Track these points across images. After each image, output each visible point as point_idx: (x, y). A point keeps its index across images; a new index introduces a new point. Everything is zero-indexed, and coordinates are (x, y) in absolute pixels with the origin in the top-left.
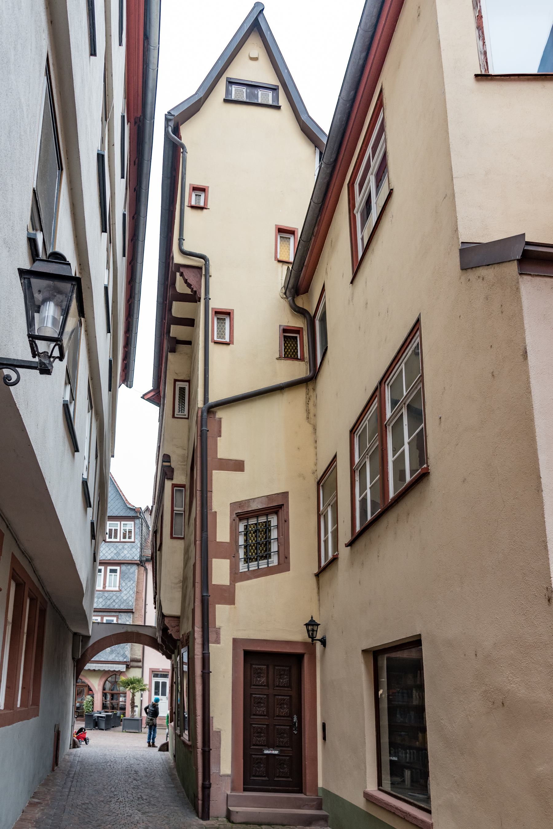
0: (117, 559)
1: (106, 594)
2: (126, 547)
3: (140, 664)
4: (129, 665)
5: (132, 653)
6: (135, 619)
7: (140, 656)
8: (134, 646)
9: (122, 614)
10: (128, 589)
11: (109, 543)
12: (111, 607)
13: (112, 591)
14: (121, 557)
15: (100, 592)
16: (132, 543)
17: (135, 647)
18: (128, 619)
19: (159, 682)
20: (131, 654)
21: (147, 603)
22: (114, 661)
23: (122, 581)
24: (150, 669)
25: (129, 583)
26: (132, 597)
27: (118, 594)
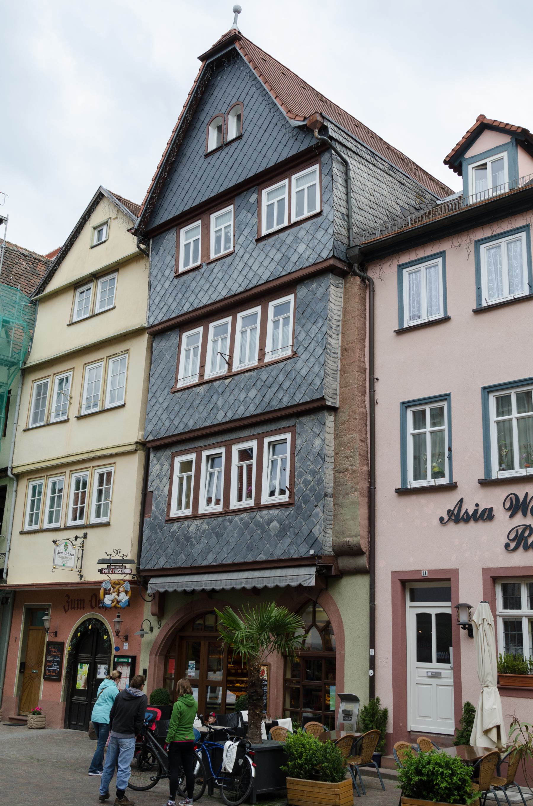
0: (284, 273)
2: (302, 233)
3: (363, 561)
7: (356, 536)
9: (303, 419)
11: (266, 241)
12: (275, 405)
13: (277, 362)
14: (291, 265)
15: (252, 373)
16: (316, 220)
17: (342, 512)
18: (317, 432)
19: (430, 615)
20: (336, 534)
21: (376, 376)
22: (286, 557)
23: (299, 329)
24: (393, 572)
25: (314, 327)
27: (289, 366)
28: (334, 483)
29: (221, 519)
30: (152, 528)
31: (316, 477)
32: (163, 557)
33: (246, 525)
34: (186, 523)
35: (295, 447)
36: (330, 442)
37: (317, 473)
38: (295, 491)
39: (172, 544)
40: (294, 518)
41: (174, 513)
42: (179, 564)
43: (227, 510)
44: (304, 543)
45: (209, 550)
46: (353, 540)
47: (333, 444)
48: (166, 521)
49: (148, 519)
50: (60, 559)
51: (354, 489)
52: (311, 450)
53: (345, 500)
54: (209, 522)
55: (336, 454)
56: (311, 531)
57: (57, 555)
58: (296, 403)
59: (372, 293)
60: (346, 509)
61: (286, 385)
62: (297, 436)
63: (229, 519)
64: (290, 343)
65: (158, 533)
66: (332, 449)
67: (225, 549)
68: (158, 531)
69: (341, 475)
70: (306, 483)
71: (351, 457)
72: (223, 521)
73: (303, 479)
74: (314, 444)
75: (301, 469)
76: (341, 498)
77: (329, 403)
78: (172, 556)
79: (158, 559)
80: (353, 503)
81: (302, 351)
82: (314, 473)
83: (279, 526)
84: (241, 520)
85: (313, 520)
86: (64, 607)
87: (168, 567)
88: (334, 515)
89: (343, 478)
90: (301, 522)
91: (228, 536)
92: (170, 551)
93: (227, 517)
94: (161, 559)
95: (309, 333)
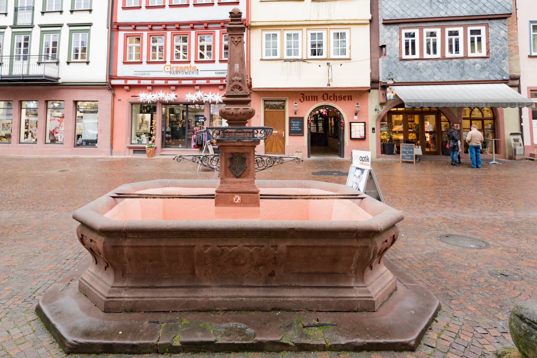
29: (440, 61)
30: (388, 63)
34: (416, 61)
45: (434, 74)
49: (385, 58)
65: (393, 65)
68: (393, 64)
73: (494, 47)
78: (407, 77)
82: (501, 45)
86: (300, 100)
87: (405, 81)
93: (444, 61)
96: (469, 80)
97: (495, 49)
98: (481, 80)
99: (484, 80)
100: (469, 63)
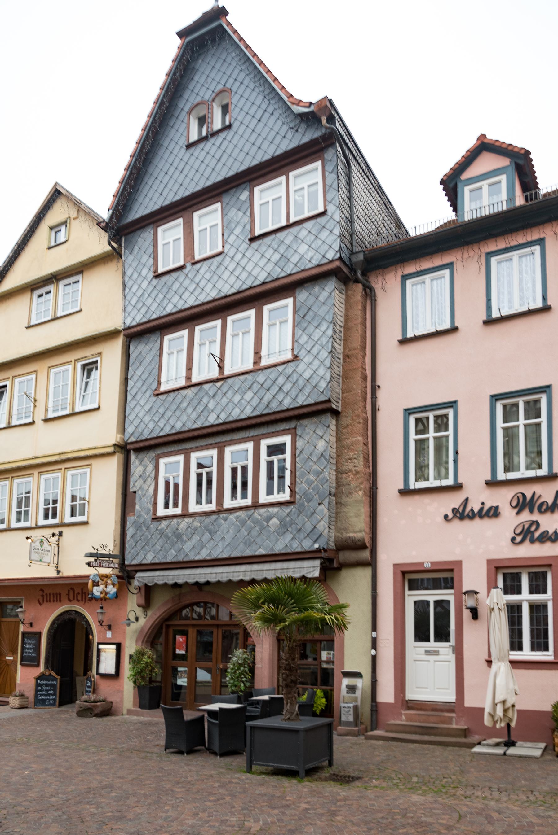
1: (261, 377)
4: (331, 560)
5: (339, 524)
6: (344, 431)
8: (345, 505)
9: (305, 422)
10: (315, 351)
12: (274, 407)
13: (275, 366)
17: (346, 510)
18: (321, 434)
23: (300, 332)
26: (325, 366)
27: (290, 369)
28: (337, 483)
29: (214, 517)
31: (320, 477)
32: (151, 553)
33: (243, 523)
34: (175, 521)
35: (296, 449)
36: (333, 445)
37: (321, 473)
38: (297, 490)
39: (160, 541)
40: (296, 515)
41: (161, 511)
42: (169, 559)
43: (220, 508)
44: (308, 538)
46: (358, 536)
47: (335, 446)
48: (153, 519)
50: (36, 555)
51: (358, 489)
52: (313, 451)
53: (348, 499)
54: (201, 520)
55: (338, 456)
56: (315, 527)
57: (33, 551)
58: (298, 405)
59: (373, 302)
60: (349, 507)
61: (286, 388)
62: (298, 437)
63: (223, 517)
64: (290, 346)
65: (143, 531)
66: (335, 451)
67: (220, 544)
69: (344, 476)
70: (310, 483)
71: (355, 458)
72: (217, 519)
73: (305, 479)
74: (317, 445)
75: (303, 469)
76: (343, 497)
77: (334, 406)
78: (161, 552)
79: (145, 555)
80: (356, 501)
81: (304, 354)
83: (279, 523)
84: (237, 518)
85: (316, 517)
87: (157, 561)
88: (337, 513)
89: (346, 479)
90: (304, 519)
91: (223, 533)
92: (158, 547)
93: (221, 516)
94: (149, 555)
95: (312, 337)
96: (257, 553)
97: (305, 482)
98: (277, 552)
99: (283, 552)
100: (260, 517)
